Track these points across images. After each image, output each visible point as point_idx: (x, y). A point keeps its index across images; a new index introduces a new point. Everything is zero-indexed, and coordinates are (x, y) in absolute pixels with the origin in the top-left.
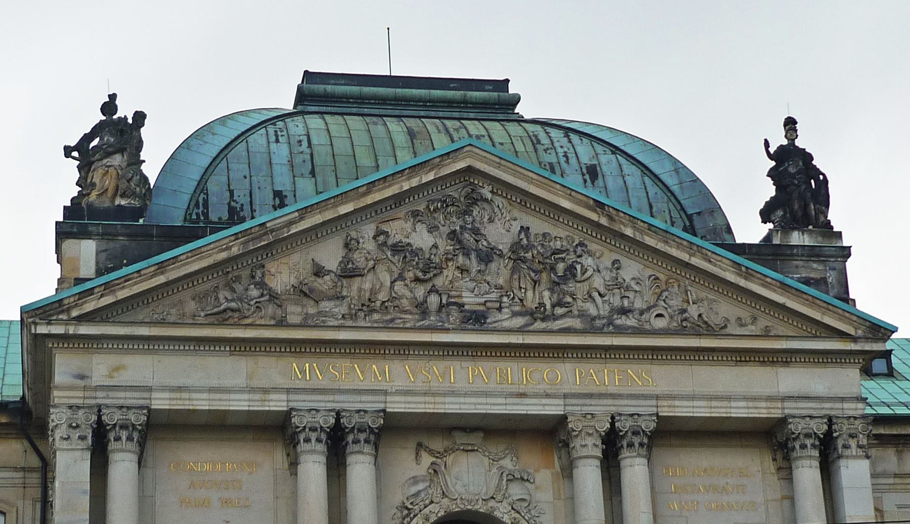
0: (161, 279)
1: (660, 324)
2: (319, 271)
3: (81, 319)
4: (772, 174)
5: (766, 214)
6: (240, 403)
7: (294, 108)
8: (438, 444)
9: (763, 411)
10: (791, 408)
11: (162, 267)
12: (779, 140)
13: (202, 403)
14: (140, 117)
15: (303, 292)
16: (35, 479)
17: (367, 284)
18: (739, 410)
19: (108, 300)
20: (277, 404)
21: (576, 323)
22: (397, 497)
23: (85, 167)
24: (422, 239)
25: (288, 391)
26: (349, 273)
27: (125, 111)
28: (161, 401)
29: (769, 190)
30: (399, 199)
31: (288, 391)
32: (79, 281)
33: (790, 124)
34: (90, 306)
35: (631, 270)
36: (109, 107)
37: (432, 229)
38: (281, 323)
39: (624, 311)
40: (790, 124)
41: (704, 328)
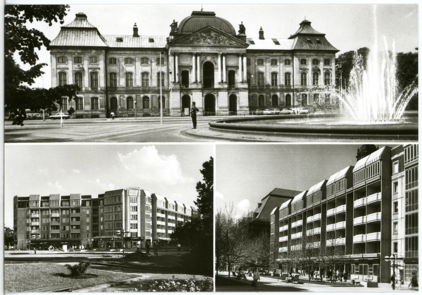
2: (195, 39)
4: (240, 28)
5: (239, 31)
7: (192, 15)
8: (206, 55)
9: (237, 52)
10: (239, 52)
12: (241, 23)
14: (177, 22)
16: (167, 55)
18: (234, 52)
22: (202, 60)
23: (172, 28)
24: (204, 35)
27: (176, 21)
29: (239, 29)
30: (202, 31)
33: (242, 22)
36: (174, 21)
37: (206, 34)
40: (242, 22)
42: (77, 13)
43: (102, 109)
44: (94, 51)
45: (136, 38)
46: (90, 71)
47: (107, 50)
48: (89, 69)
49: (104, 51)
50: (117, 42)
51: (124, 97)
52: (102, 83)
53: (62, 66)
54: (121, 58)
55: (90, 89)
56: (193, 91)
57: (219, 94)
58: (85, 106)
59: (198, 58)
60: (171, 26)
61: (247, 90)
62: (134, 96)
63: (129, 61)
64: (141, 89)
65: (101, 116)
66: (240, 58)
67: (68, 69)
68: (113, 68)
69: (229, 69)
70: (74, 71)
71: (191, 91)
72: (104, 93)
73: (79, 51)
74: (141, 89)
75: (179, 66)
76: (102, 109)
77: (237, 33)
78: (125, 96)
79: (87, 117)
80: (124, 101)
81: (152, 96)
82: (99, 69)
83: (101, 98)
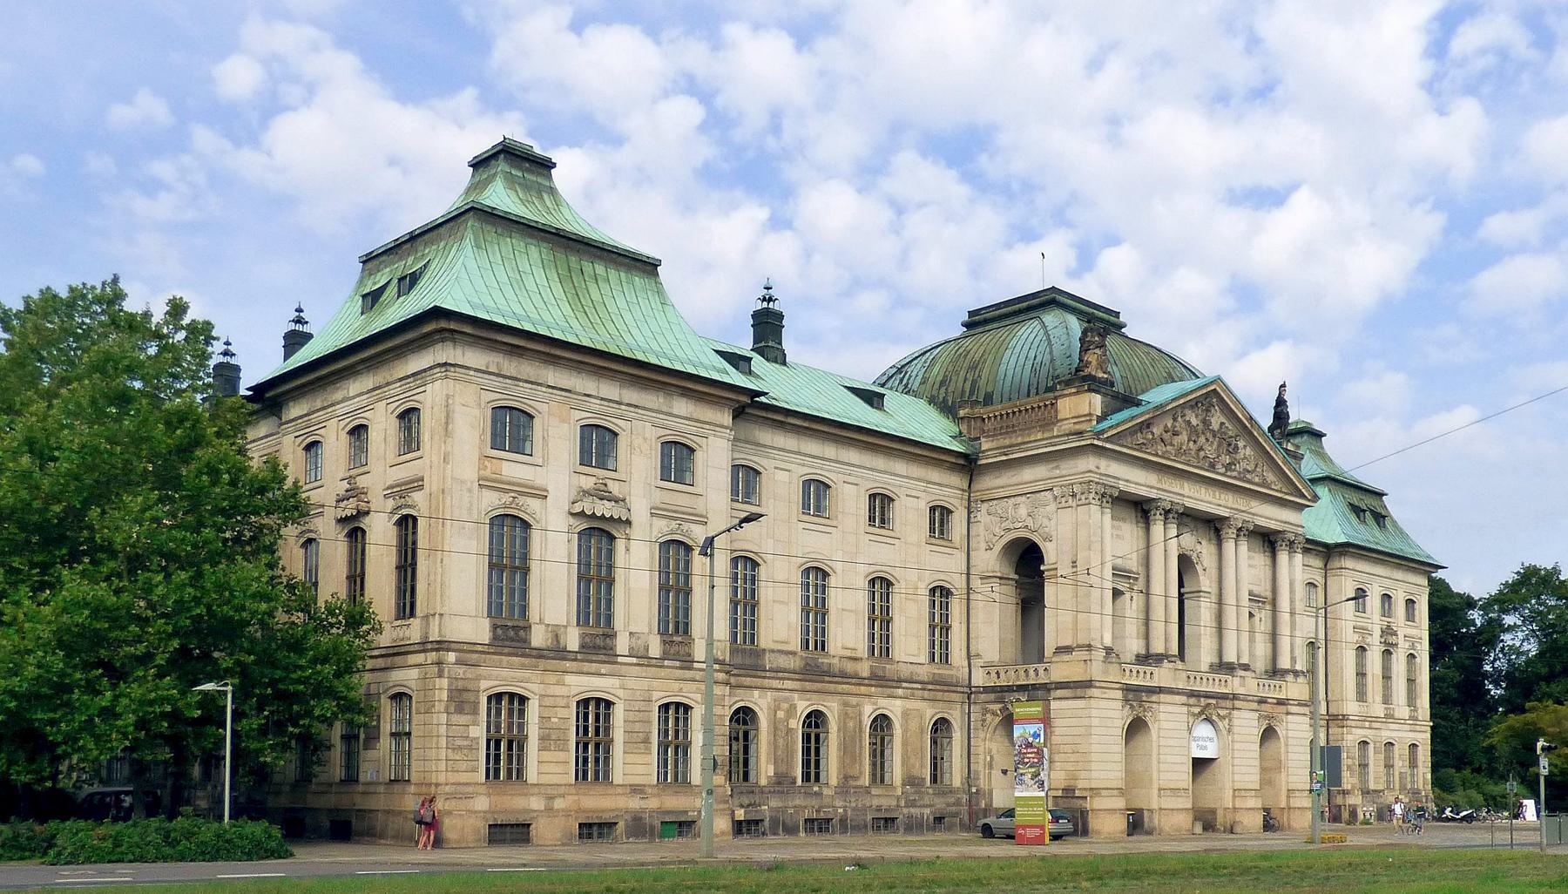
3: (1108, 440)
25: (1158, 489)
31: (1158, 489)
55: (655, 650)
56: (1163, 697)
57: (1236, 722)
58: (630, 759)
62: (831, 709)
64: (864, 669)
71: (1154, 698)
74: (864, 669)
78: (793, 707)
80: (789, 731)
81: (906, 714)
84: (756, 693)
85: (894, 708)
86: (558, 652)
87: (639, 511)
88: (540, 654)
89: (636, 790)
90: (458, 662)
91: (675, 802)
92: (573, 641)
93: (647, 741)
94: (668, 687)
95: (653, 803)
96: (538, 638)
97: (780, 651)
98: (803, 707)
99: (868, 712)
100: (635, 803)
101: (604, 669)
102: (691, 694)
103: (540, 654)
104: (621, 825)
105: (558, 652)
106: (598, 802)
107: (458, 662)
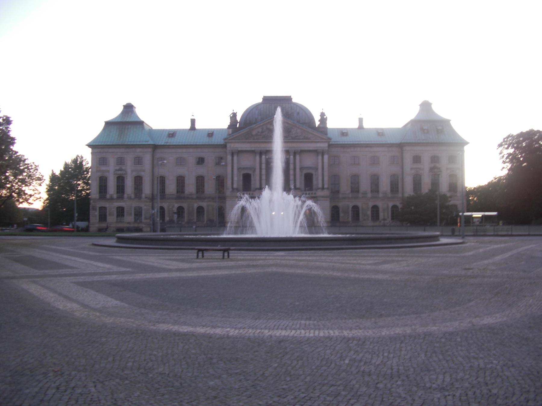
0: (239, 135)
1: (301, 138)
2: (258, 132)
3: (230, 140)
6: (249, 149)
11: (239, 133)
13: (245, 149)
15: (256, 135)
17: (264, 134)
19: (232, 137)
20: (253, 149)
21: (290, 138)
26: (262, 132)
27: (235, 112)
28: (240, 149)
29: (319, 118)
32: (230, 135)
34: (230, 138)
35: (299, 131)
38: (254, 139)
39: (297, 136)
41: (307, 138)
42: (125, 104)
43: (146, 221)
44: (139, 150)
45: (193, 131)
46: (135, 174)
47: (155, 147)
48: (132, 171)
49: (150, 150)
50: (168, 138)
51: (173, 206)
52: (147, 189)
53: (103, 168)
54: (170, 157)
55: (133, 196)
59: (263, 157)
60: (231, 118)
61: (328, 199)
62: (185, 205)
63: (180, 162)
65: (144, 229)
66: (320, 157)
67: (108, 171)
68: (161, 171)
69: (305, 171)
70: (115, 174)
72: (148, 201)
73: (122, 150)
74: (195, 197)
75: (239, 169)
76: (146, 221)
77: (317, 123)
79: (129, 230)
82: (144, 171)
83: (145, 207)
84: (164, 203)
85: (204, 204)
86: (112, 199)
87: (129, 171)
88: (108, 199)
89: (129, 223)
90: (93, 202)
91: (136, 225)
92: (115, 196)
93: (131, 214)
94: (135, 204)
95: (132, 225)
96: (108, 196)
97: (171, 194)
98: (176, 205)
99: (196, 206)
100: (128, 225)
101: (122, 201)
102: (142, 205)
103: (108, 199)
104: (125, 229)
105: (112, 199)
106: (120, 225)
107: (93, 202)
